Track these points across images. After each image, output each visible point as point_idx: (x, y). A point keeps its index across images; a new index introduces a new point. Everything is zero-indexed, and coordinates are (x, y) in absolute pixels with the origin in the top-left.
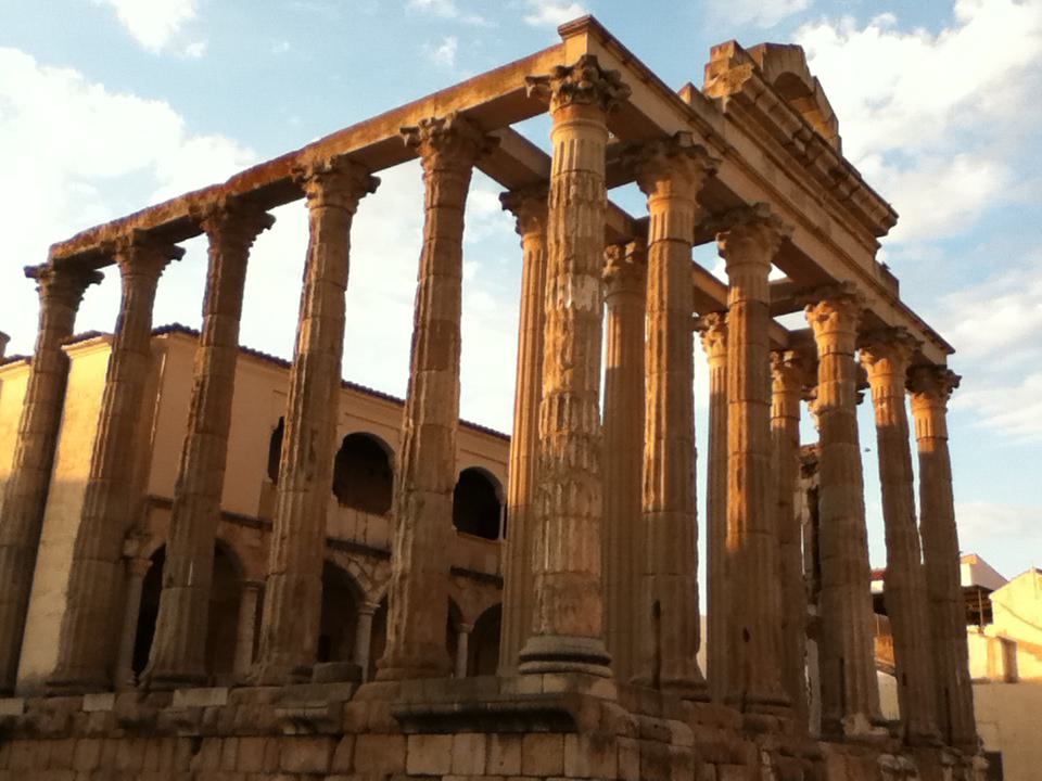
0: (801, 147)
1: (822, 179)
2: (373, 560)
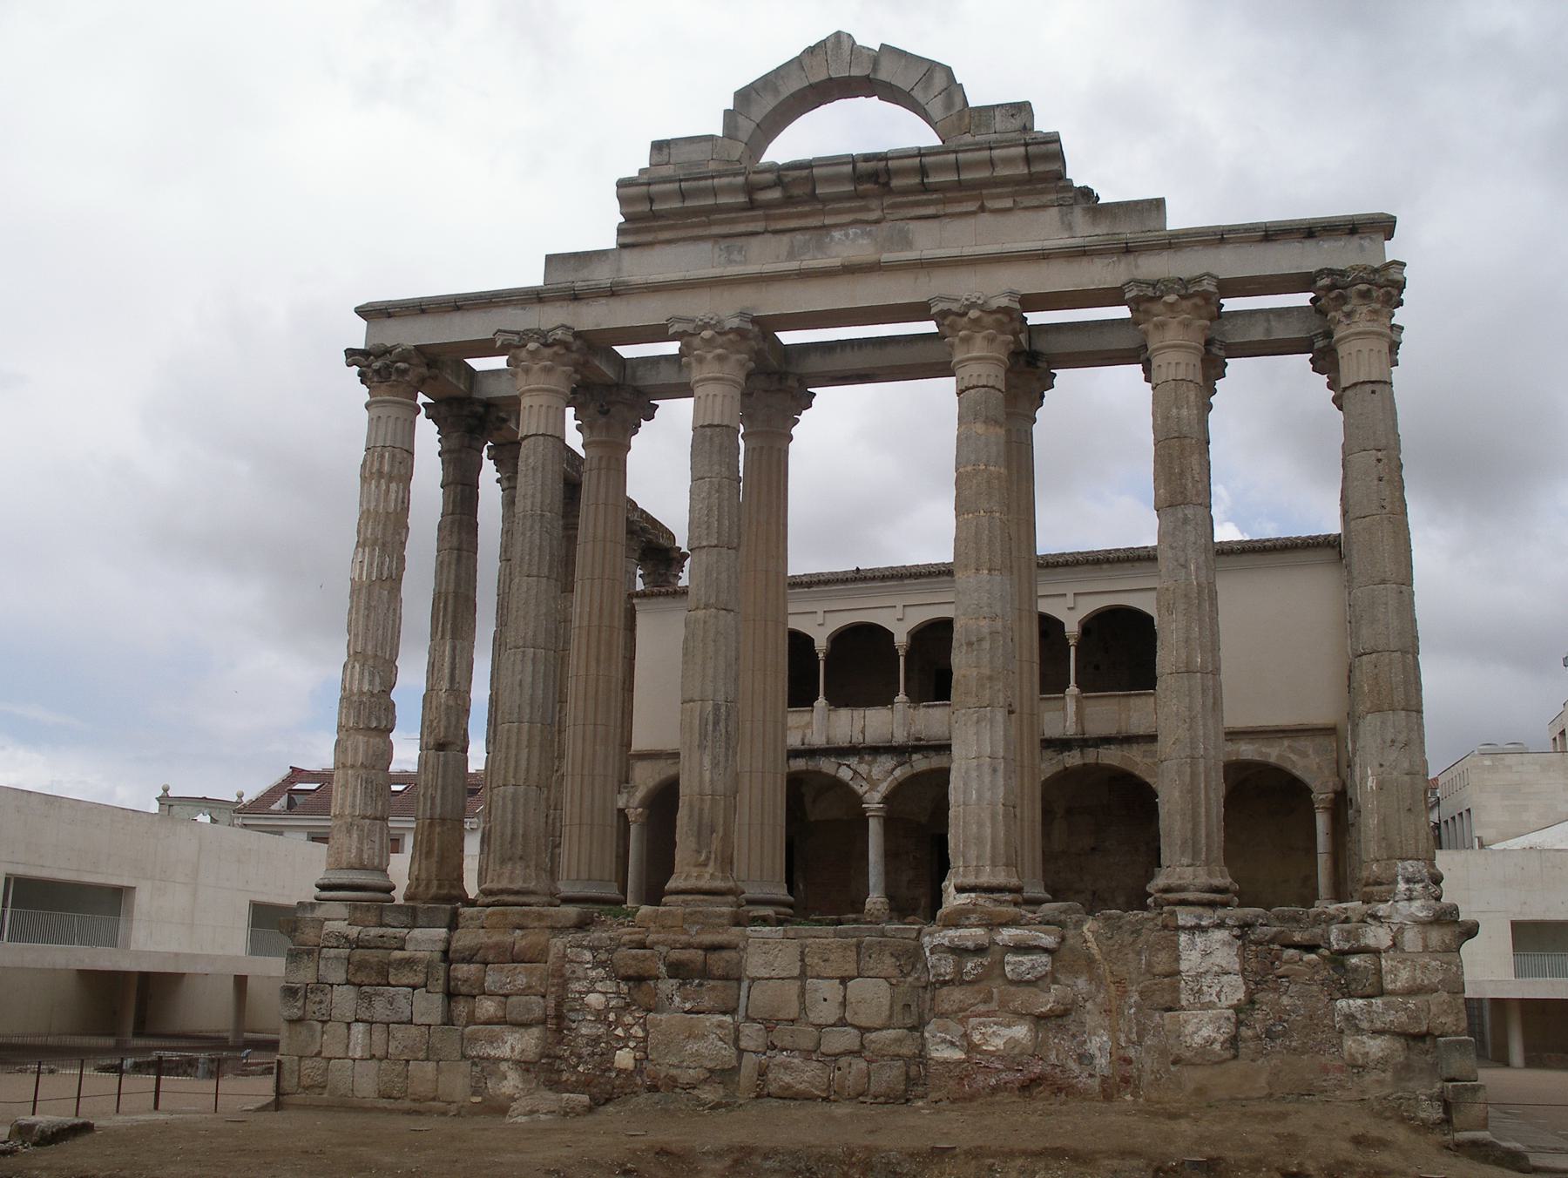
0: (775, 194)
1: (856, 196)
2: (867, 758)
